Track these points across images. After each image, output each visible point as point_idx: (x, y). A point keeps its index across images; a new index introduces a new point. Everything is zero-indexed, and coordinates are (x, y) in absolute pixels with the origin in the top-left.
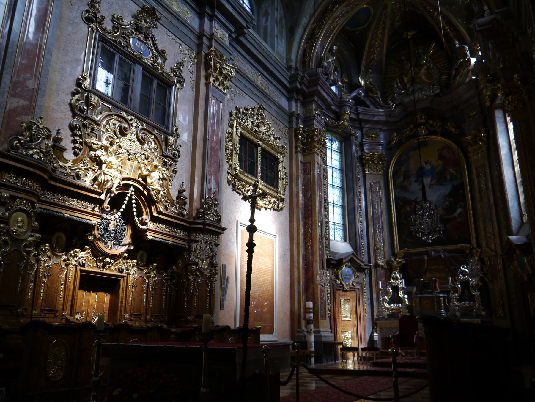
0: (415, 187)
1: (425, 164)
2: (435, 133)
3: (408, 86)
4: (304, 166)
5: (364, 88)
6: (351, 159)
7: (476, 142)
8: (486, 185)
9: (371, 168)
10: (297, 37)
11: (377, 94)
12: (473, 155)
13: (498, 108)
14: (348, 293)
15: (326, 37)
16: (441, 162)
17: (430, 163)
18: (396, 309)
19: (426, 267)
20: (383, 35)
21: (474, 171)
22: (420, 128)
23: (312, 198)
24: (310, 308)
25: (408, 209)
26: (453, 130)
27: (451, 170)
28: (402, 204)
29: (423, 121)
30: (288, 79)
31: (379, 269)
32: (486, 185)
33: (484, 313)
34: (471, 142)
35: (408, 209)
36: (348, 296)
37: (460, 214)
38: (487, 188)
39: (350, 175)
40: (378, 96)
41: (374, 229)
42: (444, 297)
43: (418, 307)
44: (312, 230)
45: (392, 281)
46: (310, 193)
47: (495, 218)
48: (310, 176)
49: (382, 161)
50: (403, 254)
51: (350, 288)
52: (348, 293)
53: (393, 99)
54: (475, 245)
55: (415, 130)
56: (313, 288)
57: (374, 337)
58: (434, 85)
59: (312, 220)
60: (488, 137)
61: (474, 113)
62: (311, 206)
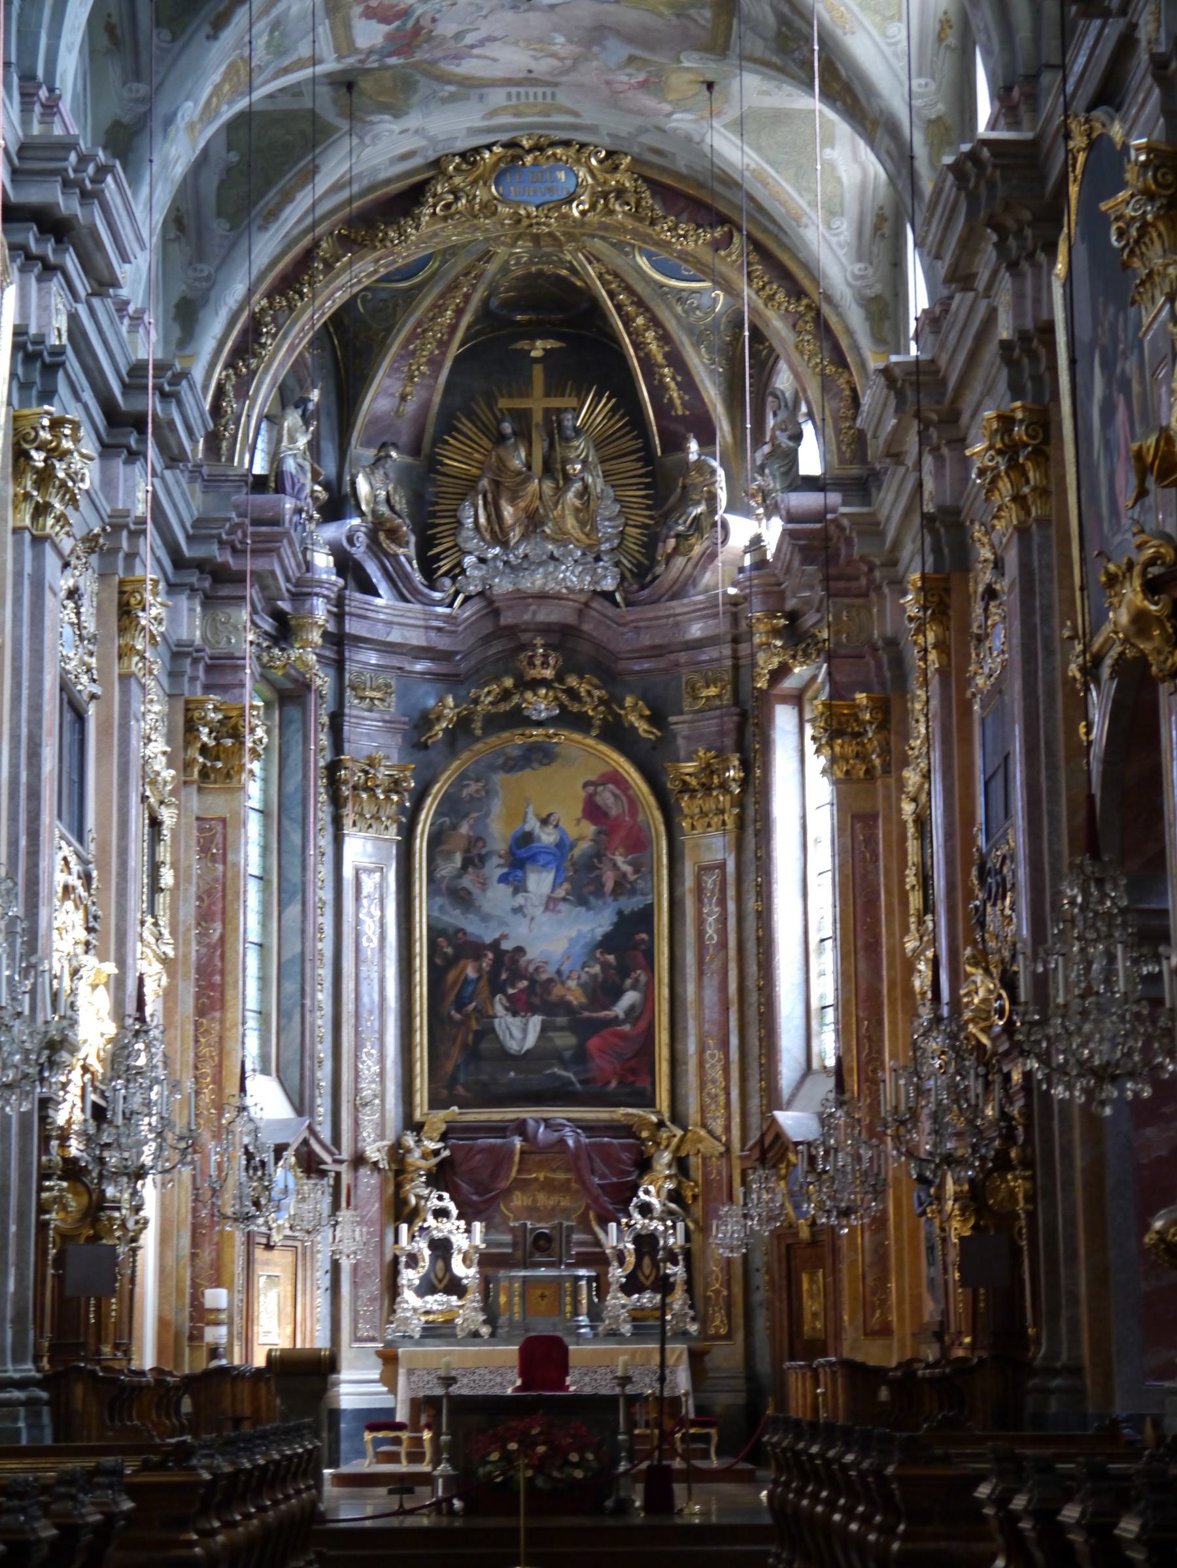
0: (497, 897)
1: (538, 824)
2: (580, 723)
3: (514, 536)
4: (201, 830)
5: (370, 518)
6: (299, 776)
7: (707, 788)
8: (723, 931)
9: (362, 815)
10: (207, 345)
11: (407, 544)
12: (693, 827)
13: (785, 699)
14: (275, 1255)
15: (292, 348)
16: (589, 829)
17: (556, 826)
18: (441, 1312)
19: (514, 1174)
20: (453, 328)
21: (689, 882)
22: (535, 694)
23: (228, 946)
24: (218, 1310)
25: (471, 972)
26: (642, 726)
27: (619, 860)
28: (449, 950)
29: (548, 673)
30: (188, 525)
31: (364, 1171)
32: (723, 931)
33: (693, 1328)
34: (693, 782)
35: (471, 972)
36: (276, 1264)
37: (632, 1008)
38: (723, 945)
39: (296, 838)
40: (407, 553)
41: (357, 1033)
42: (590, 1280)
43: (516, 1309)
44: (221, 1054)
45: (431, 1221)
46: (218, 926)
47: (734, 1041)
48: (220, 867)
49: (397, 792)
50: (444, 1127)
51: (286, 1237)
52: (275, 1252)
53: (457, 571)
54: (666, 1115)
55: (516, 699)
56: (217, 1244)
57: (338, 1401)
58: (598, 559)
59: (222, 1022)
60: (744, 783)
61: (713, 691)
62: (222, 973)
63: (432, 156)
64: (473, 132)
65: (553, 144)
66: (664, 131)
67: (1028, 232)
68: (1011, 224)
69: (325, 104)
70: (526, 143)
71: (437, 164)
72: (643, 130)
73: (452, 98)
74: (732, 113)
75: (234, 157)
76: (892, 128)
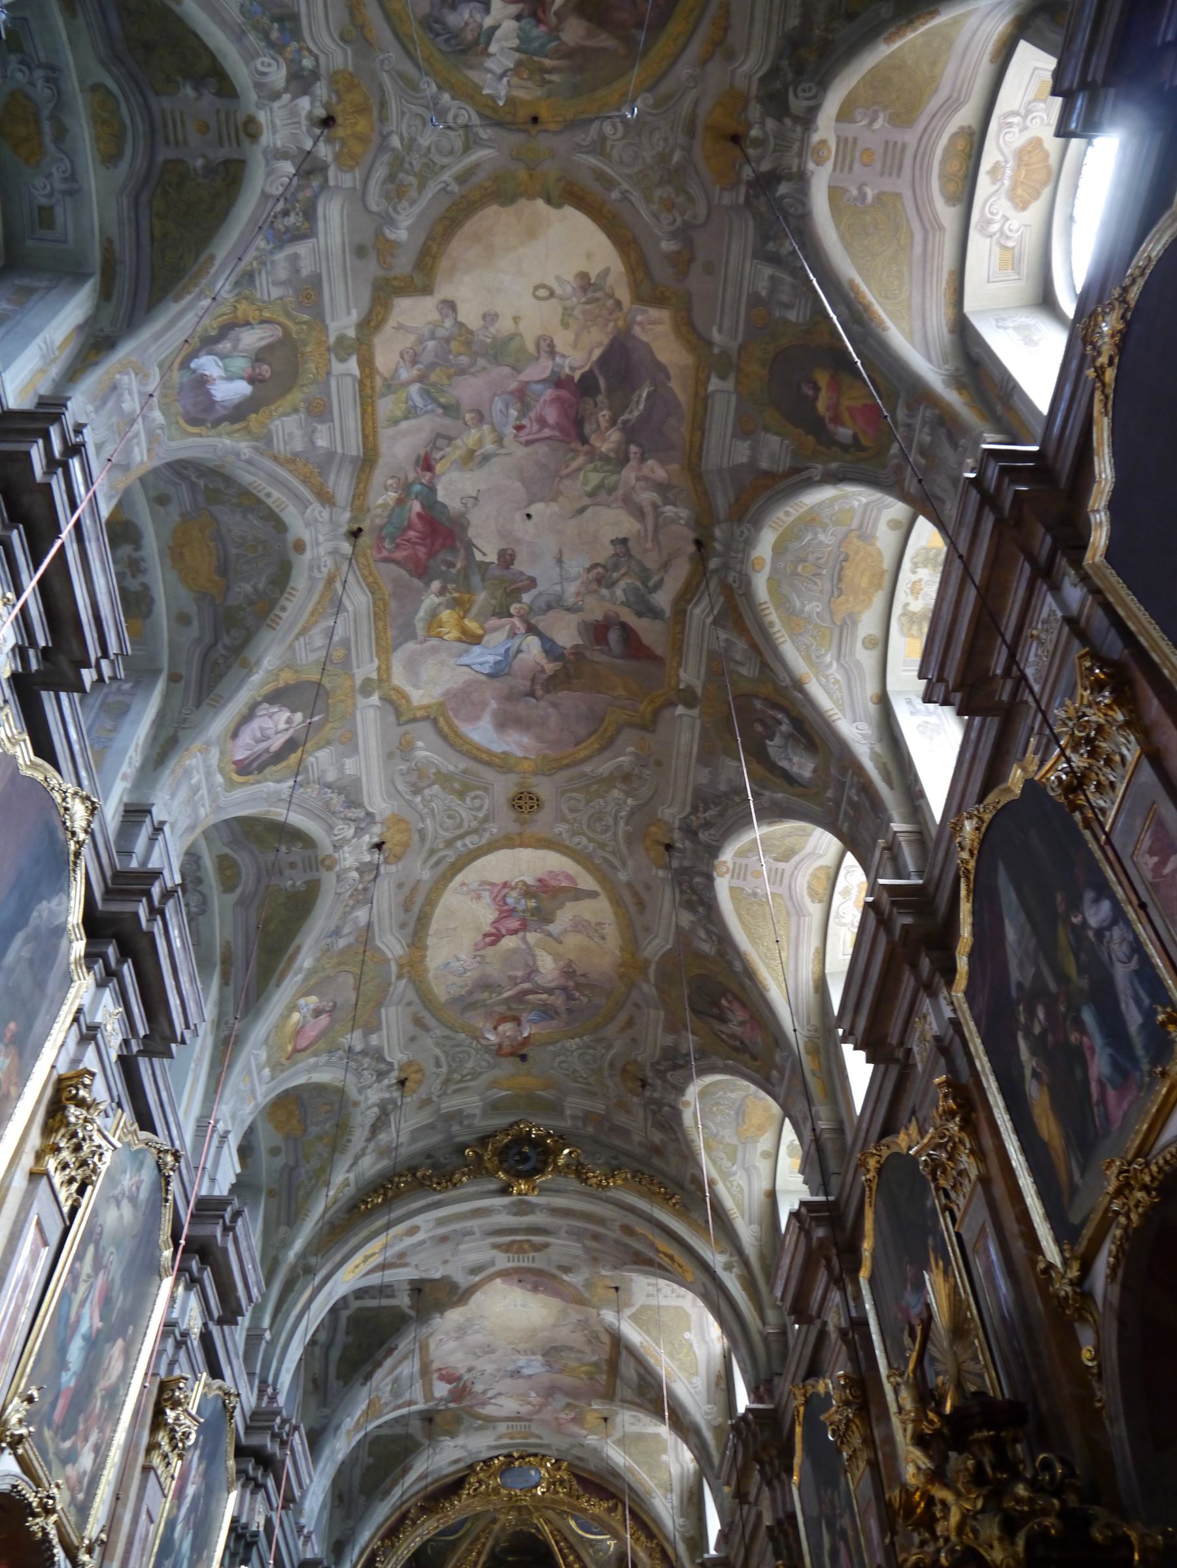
63: (469, 1462)
64: (490, 1448)
65: (529, 1455)
66: (582, 1446)
67: (776, 1462)
68: (766, 1458)
69: (416, 1427)
70: (515, 1455)
71: (471, 1467)
72: (573, 1446)
73: (480, 1428)
74: (617, 1434)
75: (371, 1461)
76: (697, 1432)
